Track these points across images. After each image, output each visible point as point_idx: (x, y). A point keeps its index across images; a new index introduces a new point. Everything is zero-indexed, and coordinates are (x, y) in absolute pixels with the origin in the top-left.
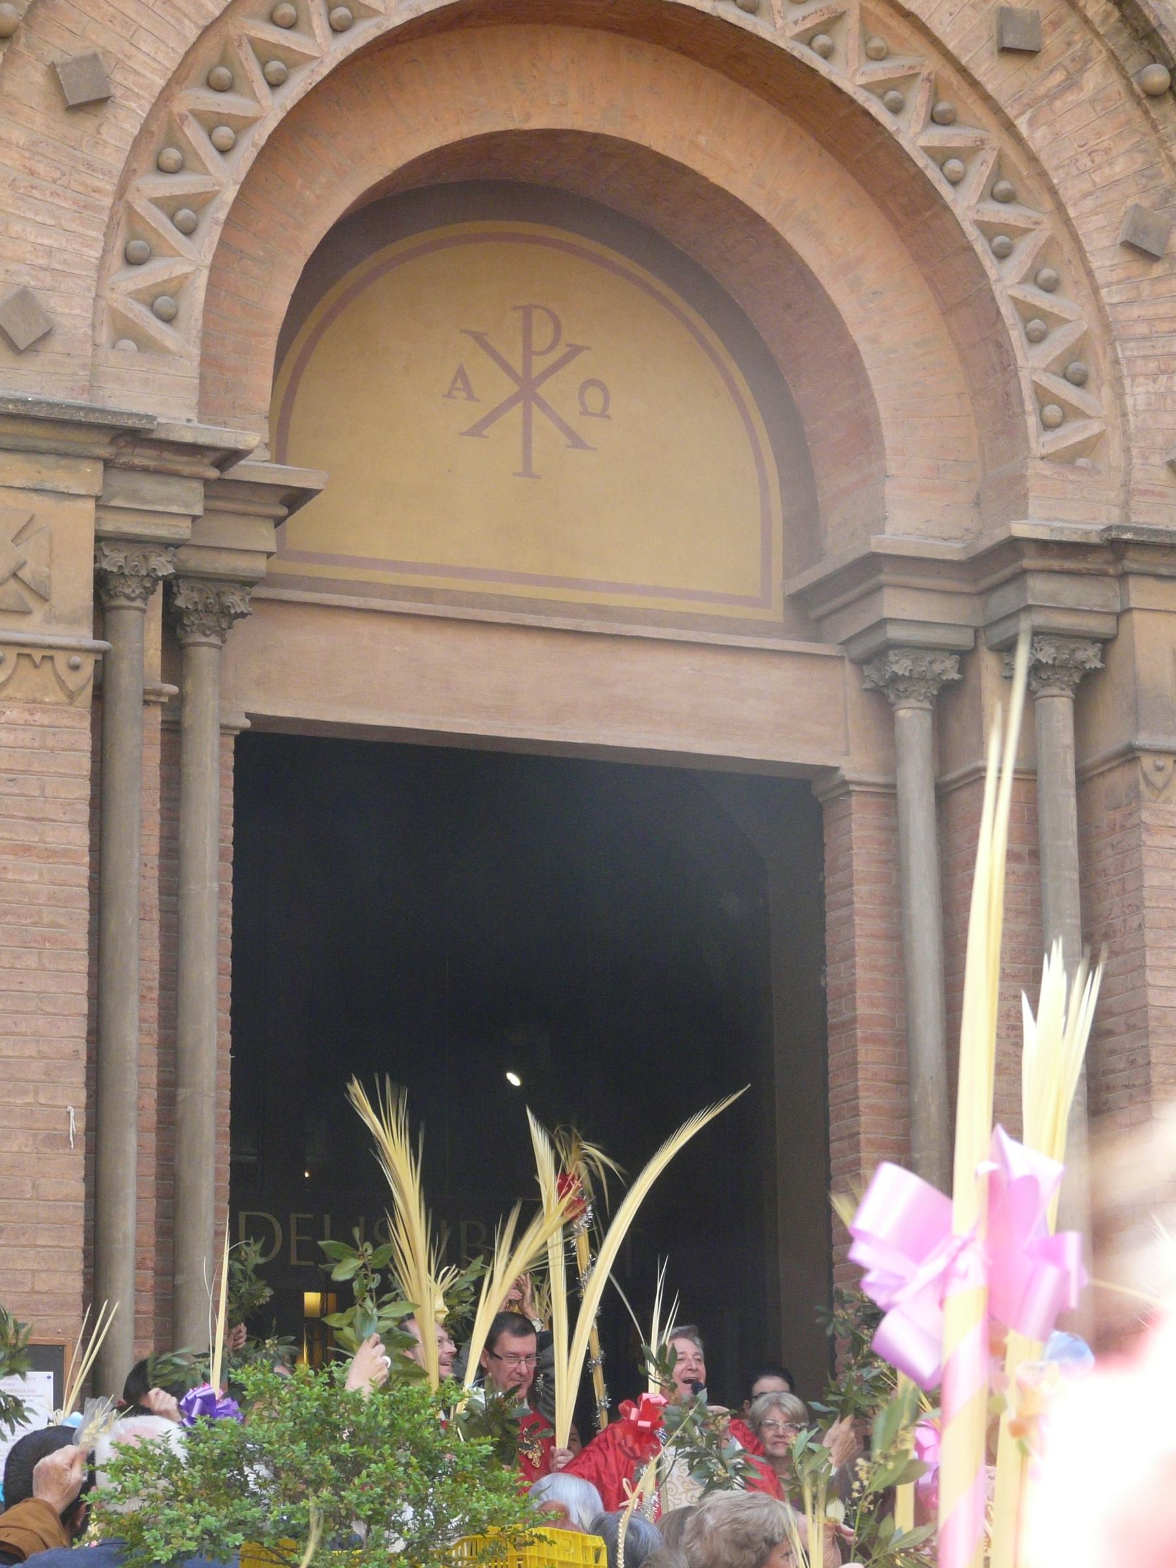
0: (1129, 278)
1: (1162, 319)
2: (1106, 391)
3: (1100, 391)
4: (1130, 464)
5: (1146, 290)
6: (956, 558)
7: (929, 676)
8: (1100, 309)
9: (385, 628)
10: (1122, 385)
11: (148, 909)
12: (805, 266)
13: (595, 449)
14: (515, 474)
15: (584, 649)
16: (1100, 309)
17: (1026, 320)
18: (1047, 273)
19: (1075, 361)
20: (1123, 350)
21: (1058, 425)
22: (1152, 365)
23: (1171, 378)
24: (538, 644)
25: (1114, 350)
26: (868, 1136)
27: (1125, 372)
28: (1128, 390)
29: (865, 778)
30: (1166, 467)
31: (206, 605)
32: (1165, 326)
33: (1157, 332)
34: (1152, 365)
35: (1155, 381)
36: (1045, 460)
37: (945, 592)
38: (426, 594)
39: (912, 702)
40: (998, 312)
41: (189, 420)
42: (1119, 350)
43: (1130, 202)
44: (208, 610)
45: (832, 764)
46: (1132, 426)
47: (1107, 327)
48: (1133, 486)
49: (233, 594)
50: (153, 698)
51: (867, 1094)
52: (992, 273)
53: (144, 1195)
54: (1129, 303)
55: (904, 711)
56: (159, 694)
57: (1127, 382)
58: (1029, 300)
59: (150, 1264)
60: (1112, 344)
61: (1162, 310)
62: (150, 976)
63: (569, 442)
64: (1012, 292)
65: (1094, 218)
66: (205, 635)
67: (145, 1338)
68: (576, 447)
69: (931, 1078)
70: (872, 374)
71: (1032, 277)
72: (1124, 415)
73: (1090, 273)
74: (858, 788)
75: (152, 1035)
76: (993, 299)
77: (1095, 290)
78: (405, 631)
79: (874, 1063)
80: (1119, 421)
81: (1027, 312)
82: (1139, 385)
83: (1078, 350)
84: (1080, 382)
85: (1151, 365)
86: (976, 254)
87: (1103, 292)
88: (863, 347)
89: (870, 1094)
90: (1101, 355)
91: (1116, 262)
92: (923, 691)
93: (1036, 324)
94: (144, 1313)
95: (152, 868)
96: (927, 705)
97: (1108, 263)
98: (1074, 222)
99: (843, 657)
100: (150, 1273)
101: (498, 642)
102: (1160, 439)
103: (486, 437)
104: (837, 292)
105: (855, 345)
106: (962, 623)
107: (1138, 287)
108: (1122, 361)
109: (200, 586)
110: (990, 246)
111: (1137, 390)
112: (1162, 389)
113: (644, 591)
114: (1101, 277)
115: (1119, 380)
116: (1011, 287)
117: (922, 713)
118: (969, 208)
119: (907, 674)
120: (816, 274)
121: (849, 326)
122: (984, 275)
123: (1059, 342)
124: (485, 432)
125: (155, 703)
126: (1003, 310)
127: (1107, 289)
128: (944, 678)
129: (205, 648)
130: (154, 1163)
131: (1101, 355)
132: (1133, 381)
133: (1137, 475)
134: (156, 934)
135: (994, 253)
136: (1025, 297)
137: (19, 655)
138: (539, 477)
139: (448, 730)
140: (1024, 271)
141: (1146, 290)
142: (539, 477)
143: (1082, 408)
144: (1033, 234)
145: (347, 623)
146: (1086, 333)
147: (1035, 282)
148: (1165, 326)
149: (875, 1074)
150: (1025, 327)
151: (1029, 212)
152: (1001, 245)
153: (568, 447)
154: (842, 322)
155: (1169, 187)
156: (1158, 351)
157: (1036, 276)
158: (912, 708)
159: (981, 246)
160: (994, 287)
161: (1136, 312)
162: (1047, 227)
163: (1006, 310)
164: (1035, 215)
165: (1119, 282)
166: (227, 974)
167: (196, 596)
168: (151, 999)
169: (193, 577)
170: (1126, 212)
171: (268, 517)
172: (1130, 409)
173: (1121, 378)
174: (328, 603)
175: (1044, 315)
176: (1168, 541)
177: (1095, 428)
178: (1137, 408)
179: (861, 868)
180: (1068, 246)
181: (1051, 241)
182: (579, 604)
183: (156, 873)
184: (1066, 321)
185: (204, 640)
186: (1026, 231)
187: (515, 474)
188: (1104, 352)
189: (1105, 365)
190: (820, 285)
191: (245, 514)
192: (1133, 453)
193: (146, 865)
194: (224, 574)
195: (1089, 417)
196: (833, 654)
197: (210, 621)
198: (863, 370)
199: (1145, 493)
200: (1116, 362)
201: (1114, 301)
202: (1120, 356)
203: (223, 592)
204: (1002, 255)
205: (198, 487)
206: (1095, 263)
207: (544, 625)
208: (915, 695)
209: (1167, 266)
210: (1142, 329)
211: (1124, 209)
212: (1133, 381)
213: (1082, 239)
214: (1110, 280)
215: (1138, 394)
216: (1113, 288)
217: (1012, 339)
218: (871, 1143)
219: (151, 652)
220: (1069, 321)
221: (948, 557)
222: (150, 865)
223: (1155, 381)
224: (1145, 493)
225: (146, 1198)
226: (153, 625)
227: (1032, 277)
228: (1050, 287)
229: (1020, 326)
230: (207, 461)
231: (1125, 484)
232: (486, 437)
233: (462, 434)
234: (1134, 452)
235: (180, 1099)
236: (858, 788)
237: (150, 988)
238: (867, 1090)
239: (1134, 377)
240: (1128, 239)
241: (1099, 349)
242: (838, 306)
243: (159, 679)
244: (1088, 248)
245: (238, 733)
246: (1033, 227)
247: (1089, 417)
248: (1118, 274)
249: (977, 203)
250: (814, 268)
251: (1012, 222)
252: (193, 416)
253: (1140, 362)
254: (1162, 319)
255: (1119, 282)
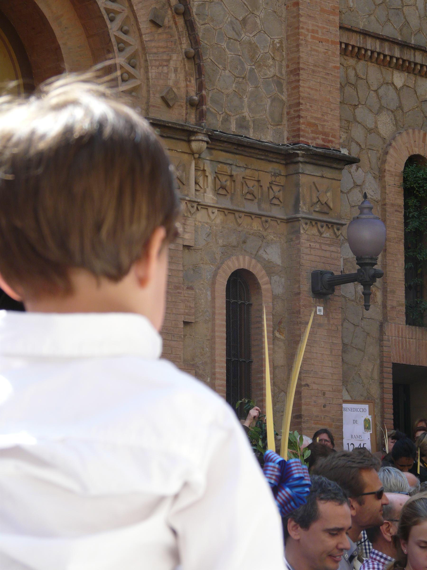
0: (151, 32)
1: (161, 47)
2: (142, 70)
3: (140, 70)
4: (150, 96)
5: (156, 37)
8: (142, 42)
10: (148, 69)
12: (45, 16)
16: (142, 42)
17: (118, 43)
18: (125, 28)
19: (133, 59)
20: (149, 56)
21: (127, 81)
22: (157, 63)
23: (163, 68)
25: (146, 56)
27: (149, 64)
28: (150, 71)
30: (160, 98)
32: (161, 50)
33: (159, 52)
34: (157, 63)
35: (158, 69)
36: (123, 92)
40: (110, 40)
42: (148, 57)
43: (153, 6)
46: (151, 83)
47: (144, 48)
48: (150, 104)
52: (109, 26)
54: (151, 41)
57: (150, 68)
58: (120, 37)
60: (145, 54)
61: (161, 44)
64: (115, 34)
65: (142, 11)
70: (64, 56)
71: (121, 29)
72: (148, 79)
73: (139, 29)
76: (109, 35)
77: (141, 35)
80: (146, 81)
81: (119, 41)
82: (153, 69)
83: (134, 56)
84: (133, 67)
85: (157, 63)
86: (104, 19)
87: (144, 36)
88: (61, 46)
90: (141, 58)
91: (148, 26)
93: (121, 45)
97: (145, 27)
98: (136, 11)
102: (159, 88)
104: (54, 26)
105: (59, 45)
107: (154, 36)
108: (148, 61)
110: (108, 16)
111: (152, 71)
112: (160, 72)
114: (143, 31)
115: (147, 68)
116: (115, 32)
118: (103, 3)
120: (48, 19)
121: (57, 38)
122: (106, 26)
123: (129, 51)
126: (112, 39)
127: (145, 36)
131: (141, 58)
132: (151, 68)
133: (152, 100)
135: (110, 19)
136: (119, 35)
137: (245, 215)
140: (119, 26)
141: (156, 37)
143: (134, 75)
144: (122, 13)
146: (137, 50)
147: (121, 31)
148: (161, 50)
150: (118, 46)
151: (121, 6)
152: (112, 16)
154: (55, 37)
155: (165, 3)
156: (159, 58)
157: (122, 29)
159: (106, 17)
160: (109, 31)
161: (153, 44)
162: (127, 12)
163: (113, 39)
164: (123, 8)
165: (148, 34)
170: (151, 10)
172: (150, 77)
173: (148, 66)
175: (125, 42)
176: (162, 124)
177: (138, 82)
178: (153, 77)
180: (132, 19)
181: (127, 17)
184: (130, 45)
186: (121, 12)
188: (142, 57)
189: (142, 61)
190: (49, 23)
192: (151, 93)
195: (136, 78)
198: (61, 54)
199: (154, 106)
200: (146, 61)
201: (147, 40)
202: (148, 59)
204: (112, 20)
206: (141, 26)
209: (163, 29)
210: (155, 50)
211: (150, 8)
212: (151, 68)
213: (138, 17)
214: (146, 32)
215: (153, 72)
216: (147, 35)
217: (114, 50)
220: (132, 45)
223: (158, 69)
224: (154, 106)
227: (121, 29)
228: (126, 33)
229: (117, 45)
231: (147, 103)
234: (151, 92)
239: (152, 66)
240: (152, 19)
241: (141, 56)
242: (54, 31)
244: (139, 21)
246: (122, 11)
247: (136, 78)
248: (148, 31)
249: (105, 1)
250: (47, 17)
251: (115, 9)
253: (154, 62)
254: (161, 47)
255: (148, 34)
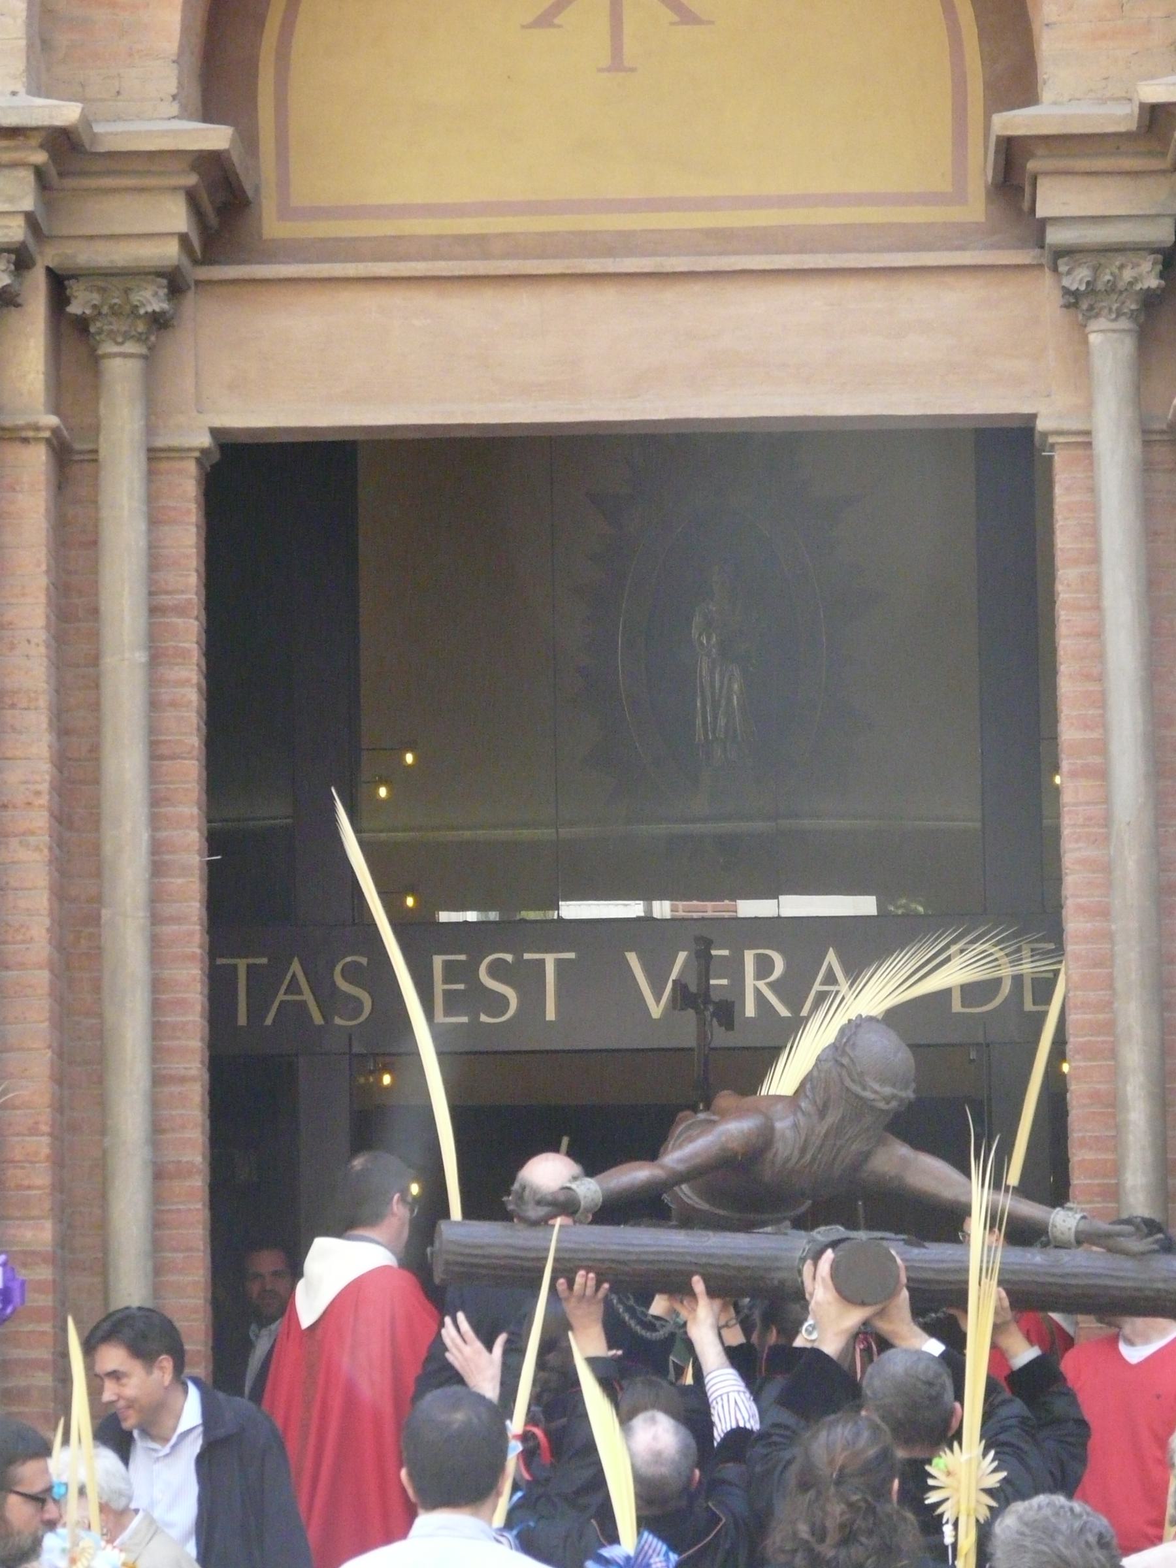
6: (1122, 128)
7: (1121, 285)
9: (397, 299)
11: (32, 695)
13: (712, 23)
14: (600, 70)
15: (670, 295)
24: (610, 295)
26: (1081, 901)
29: (1067, 425)
31: (112, 307)
37: (1128, 173)
38: (479, 245)
39: (1102, 323)
41: (14, 94)
44: (115, 312)
45: (1026, 409)
49: (146, 289)
50: (31, 434)
51: (1076, 846)
53: (34, 1046)
55: (1095, 334)
56: (37, 428)
59: (45, 1128)
62: (38, 778)
63: (676, 19)
66: (117, 344)
67: (43, 1218)
68: (683, 22)
69: (1129, 824)
74: (1061, 439)
75: (41, 851)
78: (425, 299)
79: (1088, 803)
89: (1081, 845)
92: (1115, 306)
94: (39, 1188)
95: (38, 645)
96: (1124, 324)
99: (1041, 266)
100: (46, 1140)
101: (553, 299)
103: (559, 26)
106: (1153, 212)
109: (100, 284)
113: (783, 202)
117: (1115, 335)
119: (1083, 288)
124: (557, 21)
125: (37, 439)
128: (1138, 287)
129: (118, 361)
130: (47, 1007)
134: (45, 726)
138: (633, 70)
139: (480, 422)
142: (633, 70)
145: (346, 296)
149: (1090, 819)
153: (672, 24)
158: (1101, 331)
166: (192, 758)
167: (96, 298)
168: (41, 806)
169: (93, 275)
171: (175, 189)
174: (315, 275)
179: (1069, 546)
182: (691, 231)
183: (42, 650)
185: (115, 349)
187: (600, 70)
191: (142, 190)
193: (29, 641)
194: (125, 268)
196: (1028, 261)
197: (119, 325)
203: (130, 289)
205: (29, 177)
207: (611, 269)
208: (1106, 311)
218: (1082, 909)
219: (31, 376)
221: (1110, 129)
222: (34, 640)
225: (37, 1049)
226: (32, 343)
230: (34, 142)
232: (559, 26)
233: (523, 27)
235: (103, 921)
236: (1061, 439)
237: (38, 793)
238: (1077, 841)
243: (42, 408)
245: (197, 454)
252: (20, 87)
